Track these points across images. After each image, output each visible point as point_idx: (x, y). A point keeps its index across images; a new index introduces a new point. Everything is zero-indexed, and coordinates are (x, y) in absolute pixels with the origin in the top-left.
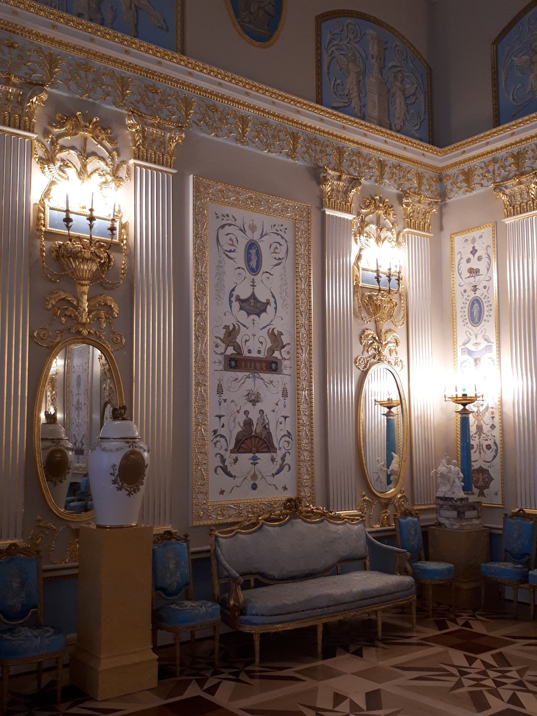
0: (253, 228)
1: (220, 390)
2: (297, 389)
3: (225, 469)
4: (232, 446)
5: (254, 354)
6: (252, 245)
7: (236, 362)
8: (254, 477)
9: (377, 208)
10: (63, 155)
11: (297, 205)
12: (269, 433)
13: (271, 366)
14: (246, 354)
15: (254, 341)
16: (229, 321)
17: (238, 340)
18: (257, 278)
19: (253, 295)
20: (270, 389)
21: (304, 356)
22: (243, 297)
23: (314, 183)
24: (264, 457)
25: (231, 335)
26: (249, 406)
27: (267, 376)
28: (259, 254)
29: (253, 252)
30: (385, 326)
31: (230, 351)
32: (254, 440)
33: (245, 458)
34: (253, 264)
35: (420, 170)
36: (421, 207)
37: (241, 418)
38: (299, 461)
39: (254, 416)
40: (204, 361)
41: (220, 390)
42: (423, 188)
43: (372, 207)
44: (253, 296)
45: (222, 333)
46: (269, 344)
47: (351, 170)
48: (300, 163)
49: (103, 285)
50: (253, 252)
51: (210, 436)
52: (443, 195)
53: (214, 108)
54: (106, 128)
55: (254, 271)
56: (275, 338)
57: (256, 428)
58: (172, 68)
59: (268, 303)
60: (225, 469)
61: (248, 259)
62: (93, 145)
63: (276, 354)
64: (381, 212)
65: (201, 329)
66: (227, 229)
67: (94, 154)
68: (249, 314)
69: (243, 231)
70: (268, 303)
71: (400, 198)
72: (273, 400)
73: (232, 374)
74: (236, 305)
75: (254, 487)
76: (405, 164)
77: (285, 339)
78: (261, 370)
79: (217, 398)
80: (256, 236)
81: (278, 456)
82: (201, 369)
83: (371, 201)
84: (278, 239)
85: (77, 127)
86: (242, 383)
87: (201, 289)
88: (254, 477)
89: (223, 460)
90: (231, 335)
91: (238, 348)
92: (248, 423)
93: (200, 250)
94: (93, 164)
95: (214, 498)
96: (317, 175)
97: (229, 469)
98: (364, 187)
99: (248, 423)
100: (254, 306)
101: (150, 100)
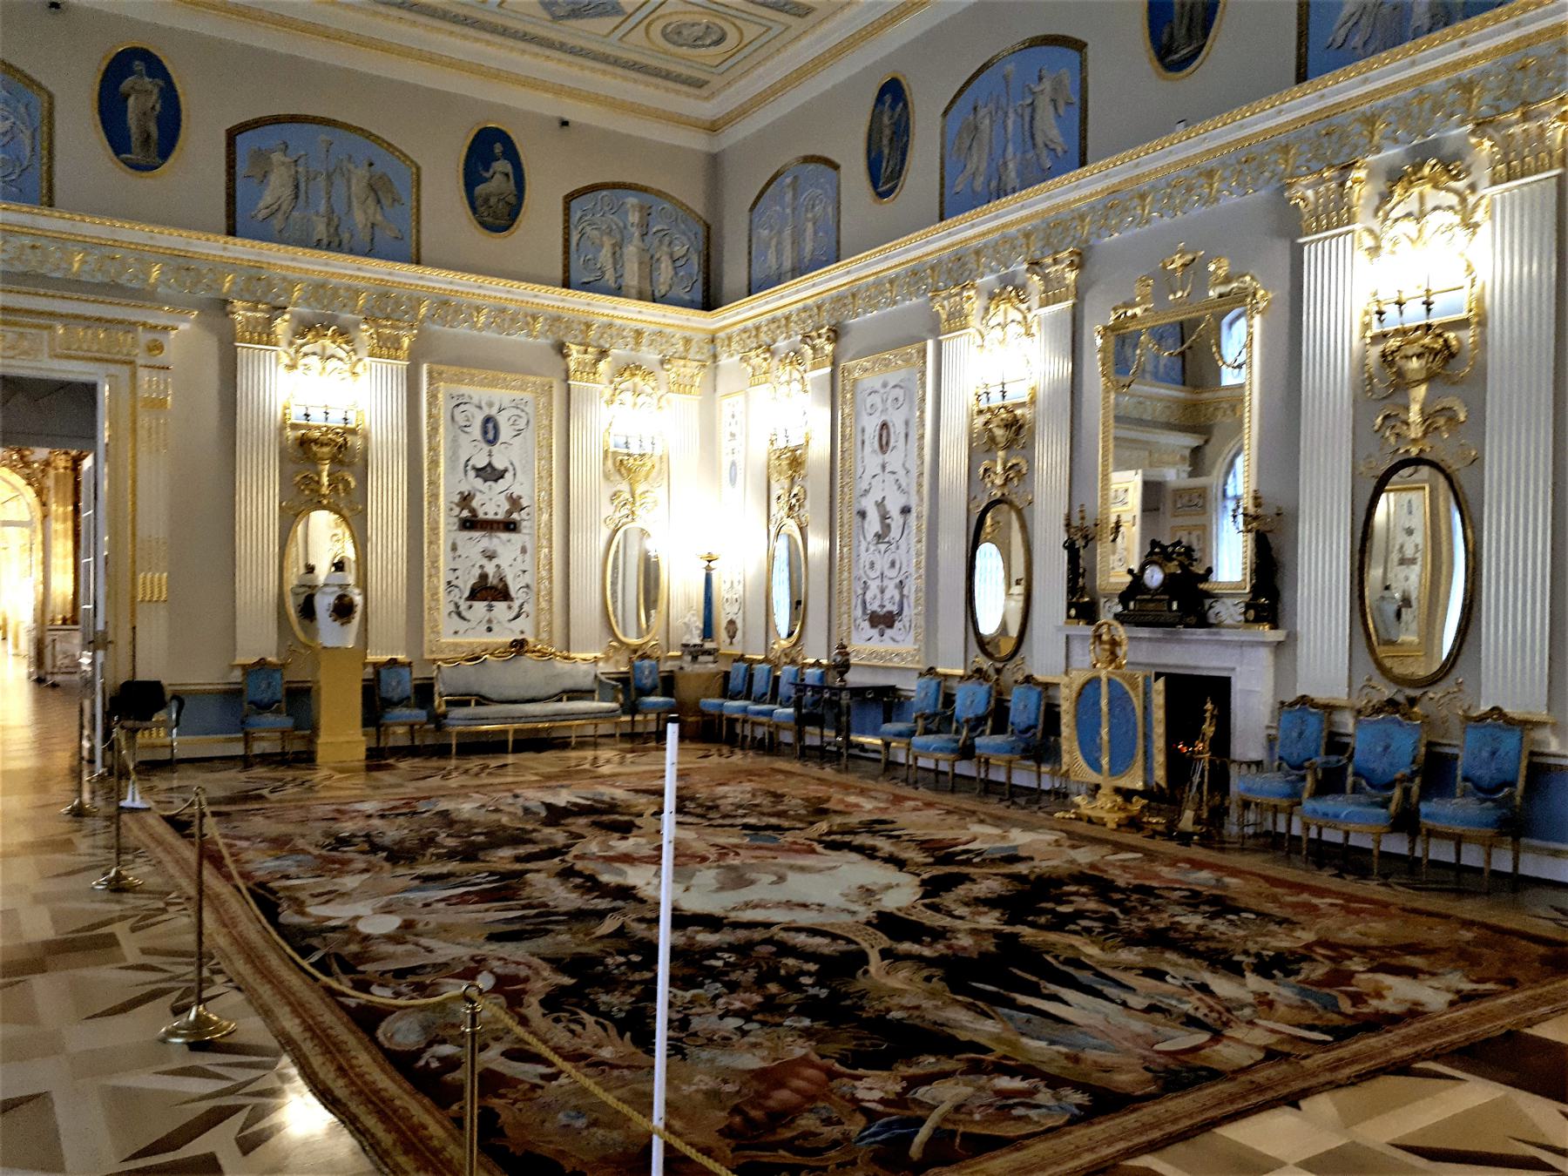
0: (491, 405)
1: (454, 548)
2: (539, 548)
3: (459, 614)
4: (467, 594)
5: (491, 516)
6: (488, 420)
7: (471, 523)
8: (490, 621)
9: (633, 375)
10: (307, 360)
11: (538, 380)
12: (506, 586)
13: (510, 526)
14: (481, 516)
15: (491, 503)
16: (465, 488)
17: (475, 504)
18: (495, 449)
19: (490, 464)
20: (506, 547)
21: (545, 517)
22: (480, 466)
23: (559, 357)
24: (500, 606)
25: (466, 500)
26: (485, 562)
27: (504, 536)
28: (496, 428)
29: (490, 426)
30: (639, 489)
31: (465, 513)
32: (489, 591)
33: (480, 606)
34: (491, 436)
35: (688, 334)
36: (688, 371)
37: (477, 572)
38: (539, 610)
39: (490, 569)
40: (437, 523)
41: (454, 548)
42: (692, 351)
43: (627, 374)
44: (490, 464)
45: (457, 499)
46: (507, 506)
47: (602, 342)
48: (541, 341)
49: (341, 463)
50: (490, 426)
51: (442, 587)
52: (715, 357)
53: (446, 303)
54: (344, 333)
55: (492, 442)
56: (515, 503)
57: (492, 581)
58: (403, 273)
59: (506, 470)
60: (459, 614)
61: (485, 432)
62: (332, 348)
63: (515, 516)
64: (637, 379)
65: (434, 496)
66: (462, 407)
67: (333, 356)
68: (486, 481)
69: (480, 407)
70: (506, 470)
71: (662, 363)
72: (508, 557)
73: (466, 534)
74: (472, 474)
75: (490, 630)
76: (668, 330)
77: (524, 503)
78: (498, 530)
79: (451, 554)
80: (494, 412)
81: (516, 605)
82: (434, 529)
83: (629, 368)
84: (518, 412)
85: (318, 336)
86: (478, 541)
87: (434, 463)
88: (490, 621)
89: (457, 607)
90: (466, 500)
91: (473, 511)
92: (484, 577)
93: (434, 430)
94: (333, 363)
95: (447, 639)
96: (561, 349)
97: (464, 614)
98: (616, 358)
99: (484, 577)
100: (490, 474)
101: (386, 308)
